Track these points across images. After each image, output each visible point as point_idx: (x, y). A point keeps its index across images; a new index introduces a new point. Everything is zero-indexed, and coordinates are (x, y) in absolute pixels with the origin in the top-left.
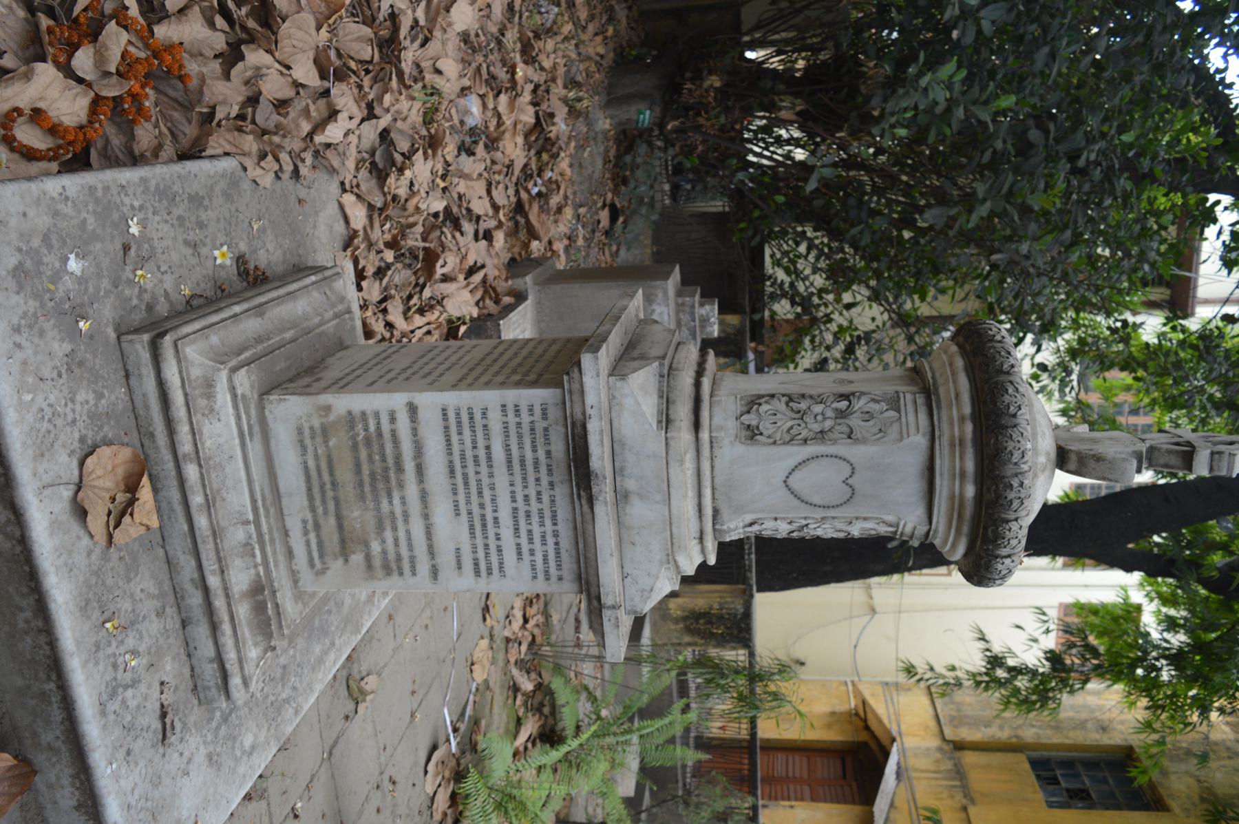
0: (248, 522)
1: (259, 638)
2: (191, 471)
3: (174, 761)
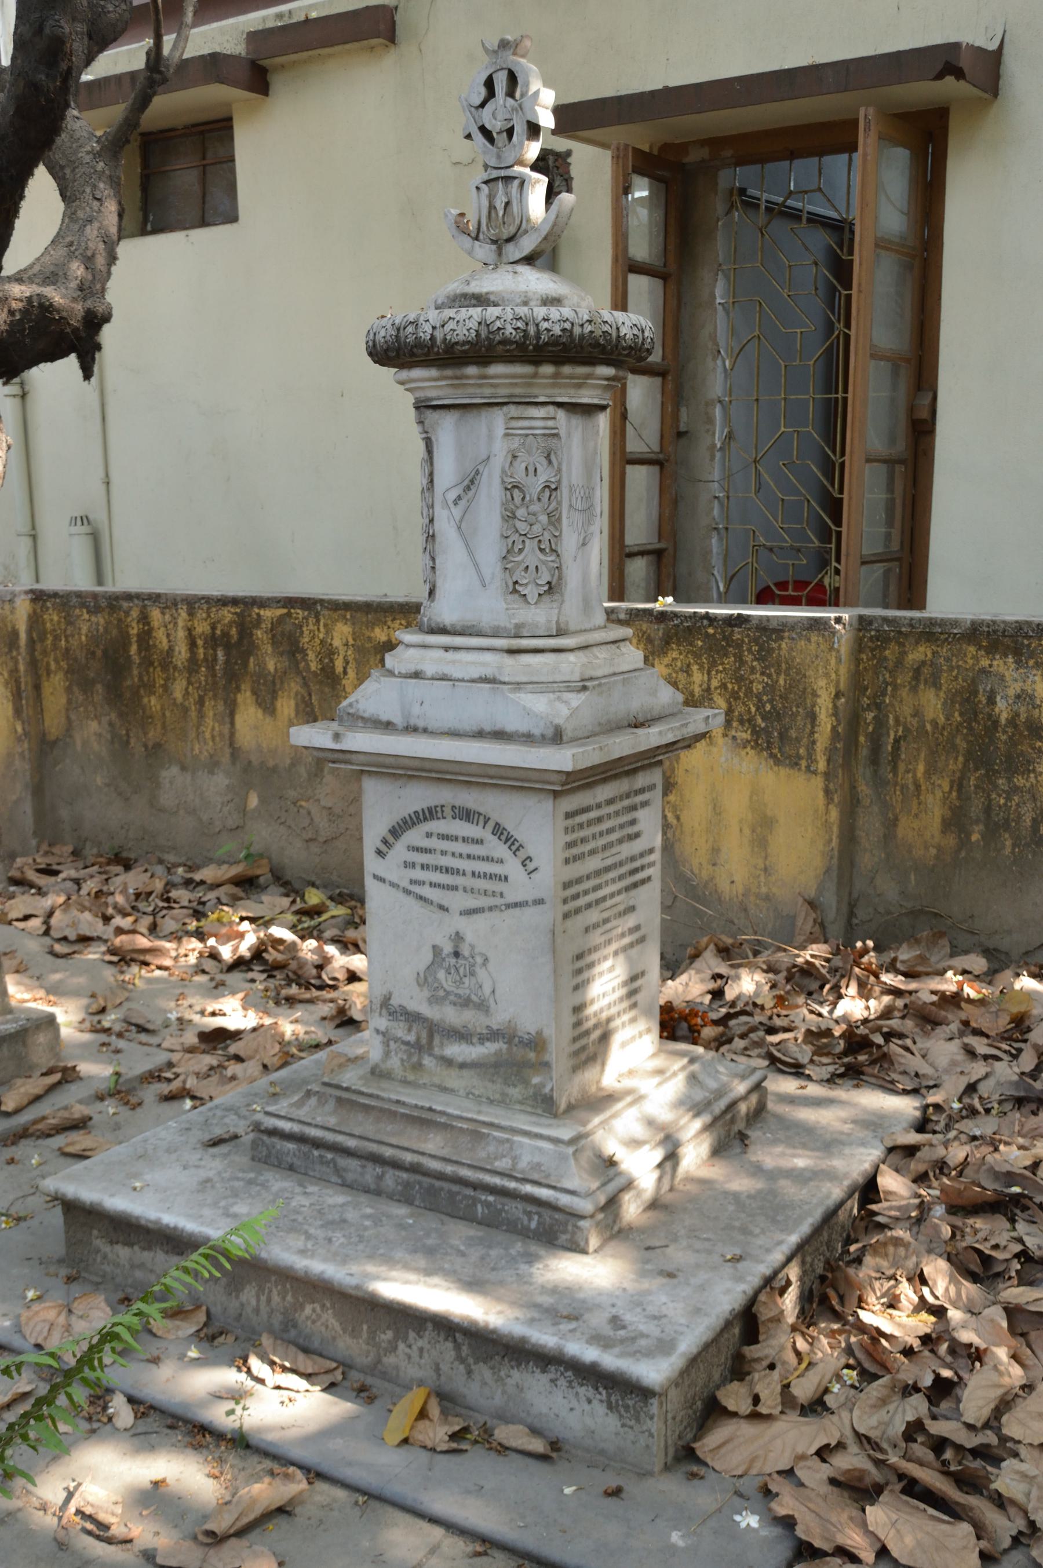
3: (194, 1157)
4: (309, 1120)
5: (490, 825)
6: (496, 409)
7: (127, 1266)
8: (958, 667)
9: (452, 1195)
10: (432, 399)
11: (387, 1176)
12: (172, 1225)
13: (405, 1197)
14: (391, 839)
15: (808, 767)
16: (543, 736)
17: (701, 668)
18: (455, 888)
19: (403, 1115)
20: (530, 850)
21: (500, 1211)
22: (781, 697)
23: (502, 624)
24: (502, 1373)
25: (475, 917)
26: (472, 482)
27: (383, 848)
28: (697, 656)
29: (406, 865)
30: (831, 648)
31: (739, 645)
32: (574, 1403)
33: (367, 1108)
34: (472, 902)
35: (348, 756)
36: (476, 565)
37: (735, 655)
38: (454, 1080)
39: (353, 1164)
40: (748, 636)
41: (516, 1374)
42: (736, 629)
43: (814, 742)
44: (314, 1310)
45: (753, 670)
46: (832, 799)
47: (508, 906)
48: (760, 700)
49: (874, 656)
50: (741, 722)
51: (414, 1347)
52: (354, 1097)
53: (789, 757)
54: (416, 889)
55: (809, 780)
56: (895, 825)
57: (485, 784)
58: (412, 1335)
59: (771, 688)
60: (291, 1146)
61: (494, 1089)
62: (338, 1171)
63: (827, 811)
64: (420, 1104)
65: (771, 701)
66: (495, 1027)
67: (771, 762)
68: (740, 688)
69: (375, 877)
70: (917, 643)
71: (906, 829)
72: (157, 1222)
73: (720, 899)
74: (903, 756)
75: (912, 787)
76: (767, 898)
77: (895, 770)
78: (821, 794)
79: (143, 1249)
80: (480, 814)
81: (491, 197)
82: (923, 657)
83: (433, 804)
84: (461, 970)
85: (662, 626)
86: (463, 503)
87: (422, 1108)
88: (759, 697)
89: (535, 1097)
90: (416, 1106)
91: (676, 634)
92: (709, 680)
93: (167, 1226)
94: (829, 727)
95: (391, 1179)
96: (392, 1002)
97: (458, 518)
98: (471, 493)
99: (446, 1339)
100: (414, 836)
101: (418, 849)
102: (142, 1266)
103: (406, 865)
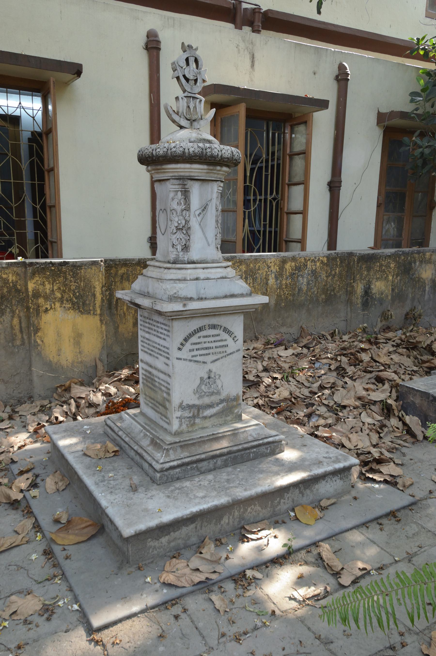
0: (142, 430)
1: (160, 451)
2: (120, 433)
4: (180, 458)
5: (223, 328)
6: (214, 182)
7: (166, 544)
8: (135, 274)
9: (242, 455)
10: (195, 177)
11: (218, 461)
12: (198, 510)
13: (226, 465)
14: (184, 343)
15: (94, 313)
16: (247, 294)
17: (49, 283)
18: (209, 354)
19: (207, 440)
20: (236, 334)
21: (258, 453)
22: (82, 290)
23: (215, 259)
24: (313, 489)
25: (216, 362)
26: (205, 208)
27: (181, 347)
28: (47, 278)
29: (190, 351)
30: (100, 271)
31: (65, 273)
32: (332, 484)
33: (193, 444)
34: (215, 357)
35: (183, 312)
36: (206, 238)
37: (63, 277)
38: (207, 423)
39: (205, 463)
40: (68, 269)
41: (317, 486)
42: (63, 267)
43: (95, 304)
44: (251, 509)
45: (71, 281)
46: (103, 323)
47: (228, 355)
48: (74, 292)
49: (108, 273)
50: (67, 301)
51: (286, 498)
52: (186, 443)
53: (87, 311)
54: (195, 359)
55: (94, 318)
56: (118, 328)
57: (208, 315)
58: (286, 494)
59: (78, 287)
60: (178, 470)
61: (221, 421)
62: (198, 470)
63: (101, 327)
64: (209, 434)
65: (78, 292)
66: (222, 399)
67: (80, 314)
68: (66, 289)
69: (177, 359)
70: (121, 267)
71: (122, 329)
72: (192, 513)
73: (62, 367)
74: (119, 305)
75: (123, 315)
76: (81, 362)
77: (117, 310)
78: (99, 321)
79: (174, 531)
80: (218, 325)
81: (187, 103)
82: (124, 272)
83: (201, 326)
84: (211, 383)
85: (31, 268)
86: (201, 216)
87: (210, 435)
88: (74, 291)
89: (236, 417)
90: (208, 436)
91: (38, 271)
92: (53, 287)
93: (197, 512)
94: (100, 298)
95: (219, 461)
96: (183, 404)
97: (199, 221)
98: (205, 212)
99: (297, 489)
100: (194, 339)
101: (195, 344)
102: (175, 539)
103: (190, 351)
